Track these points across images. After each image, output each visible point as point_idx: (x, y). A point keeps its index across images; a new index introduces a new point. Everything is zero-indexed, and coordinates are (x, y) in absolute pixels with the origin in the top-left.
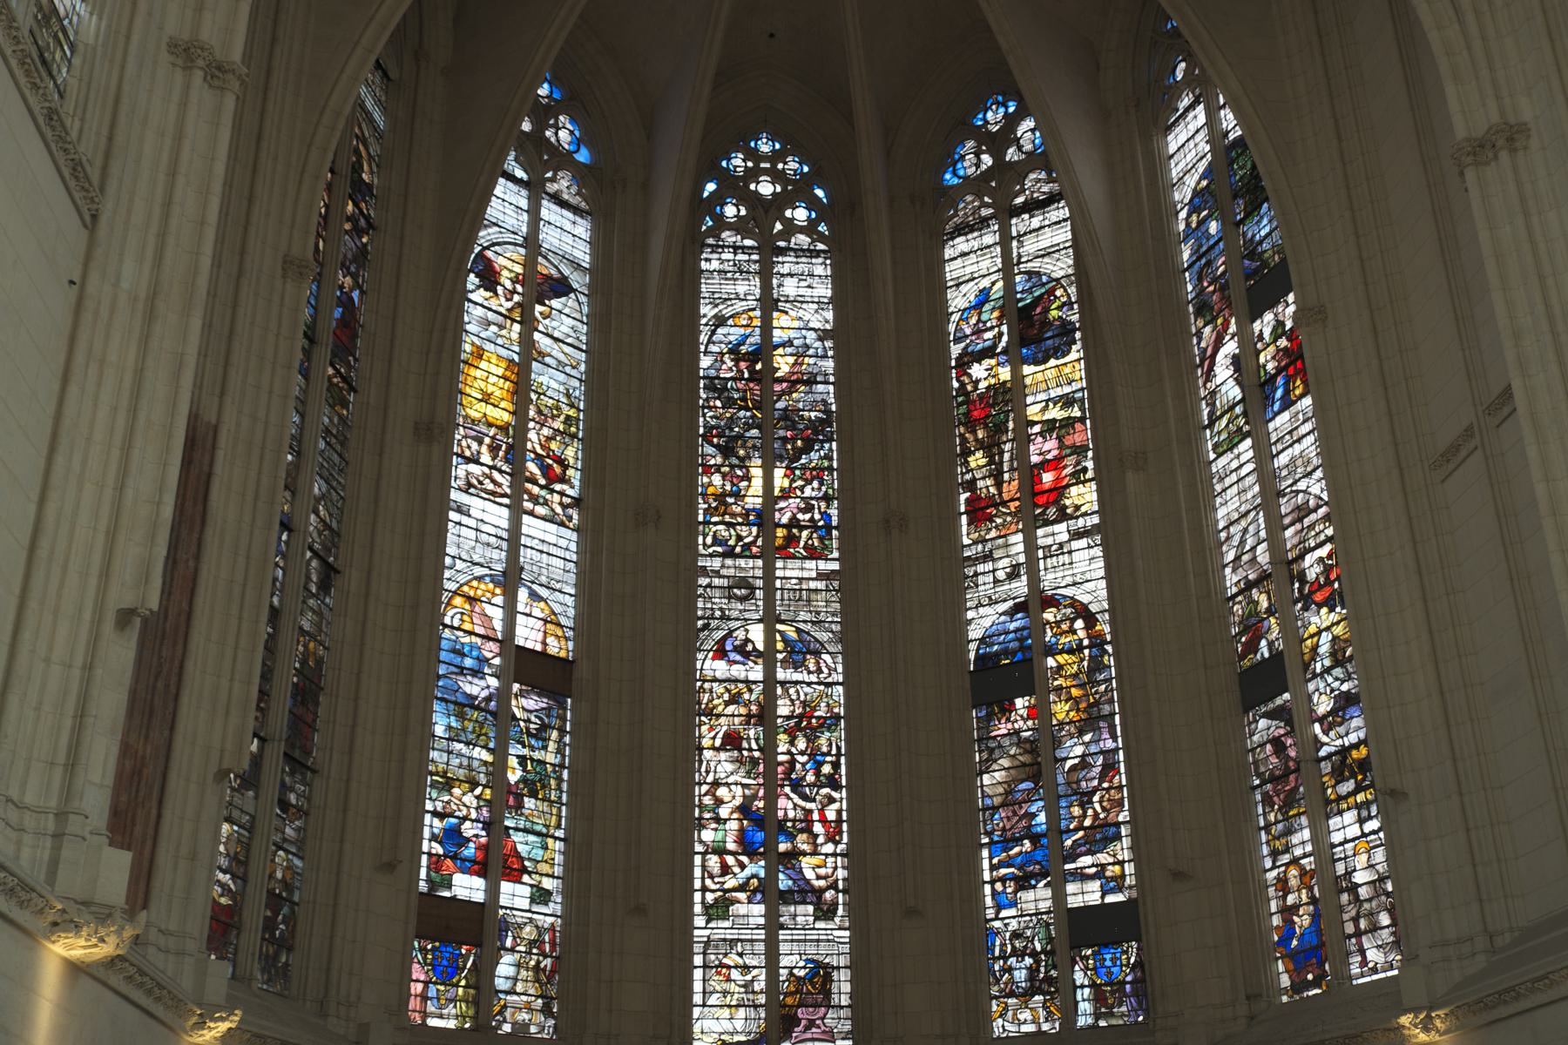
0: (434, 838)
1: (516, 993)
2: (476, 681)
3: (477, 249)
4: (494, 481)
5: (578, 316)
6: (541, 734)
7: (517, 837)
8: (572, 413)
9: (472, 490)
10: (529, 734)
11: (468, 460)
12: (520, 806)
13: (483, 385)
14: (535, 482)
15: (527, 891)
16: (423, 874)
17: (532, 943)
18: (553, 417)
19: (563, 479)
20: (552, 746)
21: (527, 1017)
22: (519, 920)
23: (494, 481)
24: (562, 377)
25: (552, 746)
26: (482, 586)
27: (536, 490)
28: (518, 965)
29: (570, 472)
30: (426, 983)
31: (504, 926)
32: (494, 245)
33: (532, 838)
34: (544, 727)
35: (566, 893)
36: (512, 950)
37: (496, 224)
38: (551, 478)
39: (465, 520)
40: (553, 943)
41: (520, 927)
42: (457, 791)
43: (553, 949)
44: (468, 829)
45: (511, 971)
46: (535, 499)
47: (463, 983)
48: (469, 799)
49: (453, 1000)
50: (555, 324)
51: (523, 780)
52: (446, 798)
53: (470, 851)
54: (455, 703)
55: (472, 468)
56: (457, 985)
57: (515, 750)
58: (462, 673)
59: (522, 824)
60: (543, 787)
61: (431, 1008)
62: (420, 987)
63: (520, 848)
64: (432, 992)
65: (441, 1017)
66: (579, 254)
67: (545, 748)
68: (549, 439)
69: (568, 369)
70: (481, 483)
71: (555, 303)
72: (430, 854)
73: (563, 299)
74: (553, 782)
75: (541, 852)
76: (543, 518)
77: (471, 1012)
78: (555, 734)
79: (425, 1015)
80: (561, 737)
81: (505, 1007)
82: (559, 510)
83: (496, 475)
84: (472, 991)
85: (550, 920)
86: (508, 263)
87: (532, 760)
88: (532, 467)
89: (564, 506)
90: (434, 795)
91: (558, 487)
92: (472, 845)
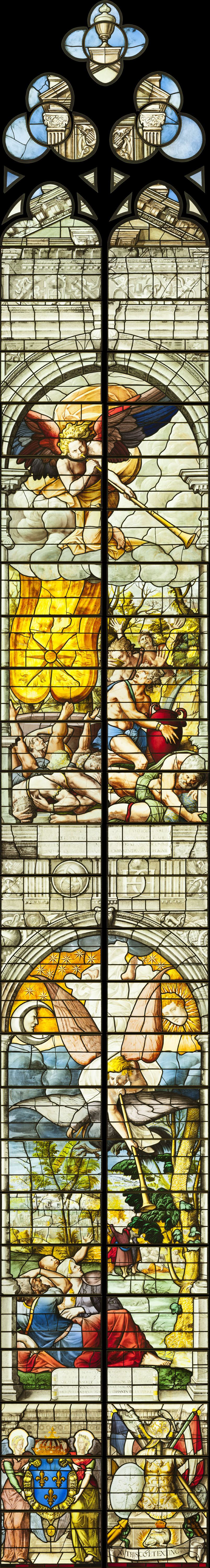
0: (20, 1328)
1: (142, 1510)
2: (65, 1100)
3: (13, 413)
4: (74, 791)
5: (192, 449)
6: (162, 1152)
7: (129, 1304)
8: (188, 626)
9: (41, 817)
10: (142, 1155)
11: (30, 773)
12: (134, 1259)
13: (42, 639)
14: (129, 767)
16: (7, 1376)
18: (156, 648)
19: (177, 746)
20: (181, 1165)
23: (74, 791)
24: (166, 573)
25: (181, 1165)
26: (64, 958)
27: (128, 779)
29: (190, 729)
30: (27, 1513)
32: (44, 391)
33: (156, 1302)
34: (166, 1141)
37: (44, 352)
38: (155, 748)
39: (31, 866)
42: (48, 1261)
43: (198, 1446)
44: (70, 1309)
46: (130, 797)
48: (67, 1266)
50: (148, 483)
51: (137, 1224)
52: (32, 1274)
53: (74, 1336)
54: (37, 1139)
55: (39, 782)
57: (118, 1182)
58: (44, 1096)
59: (137, 1288)
60: (169, 1227)
62: (18, 1518)
63: (138, 1319)
64: (35, 1521)
66: (185, 331)
67: (170, 1170)
68: (148, 687)
69: (177, 554)
70: (52, 800)
71: (148, 446)
72: (15, 1349)
73: (162, 432)
74: (184, 1216)
75: (172, 1319)
76: (147, 822)
78: (185, 1147)
80: (195, 1150)
82: (172, 800)
83: (76, 779)
85: (190, 1408)
86: (71, 413)
87: (149, 1192)
88: (123, 745)
89: (179, 790)
90: (15, 1273)
91: (169, 762)
92: (76, 1327)
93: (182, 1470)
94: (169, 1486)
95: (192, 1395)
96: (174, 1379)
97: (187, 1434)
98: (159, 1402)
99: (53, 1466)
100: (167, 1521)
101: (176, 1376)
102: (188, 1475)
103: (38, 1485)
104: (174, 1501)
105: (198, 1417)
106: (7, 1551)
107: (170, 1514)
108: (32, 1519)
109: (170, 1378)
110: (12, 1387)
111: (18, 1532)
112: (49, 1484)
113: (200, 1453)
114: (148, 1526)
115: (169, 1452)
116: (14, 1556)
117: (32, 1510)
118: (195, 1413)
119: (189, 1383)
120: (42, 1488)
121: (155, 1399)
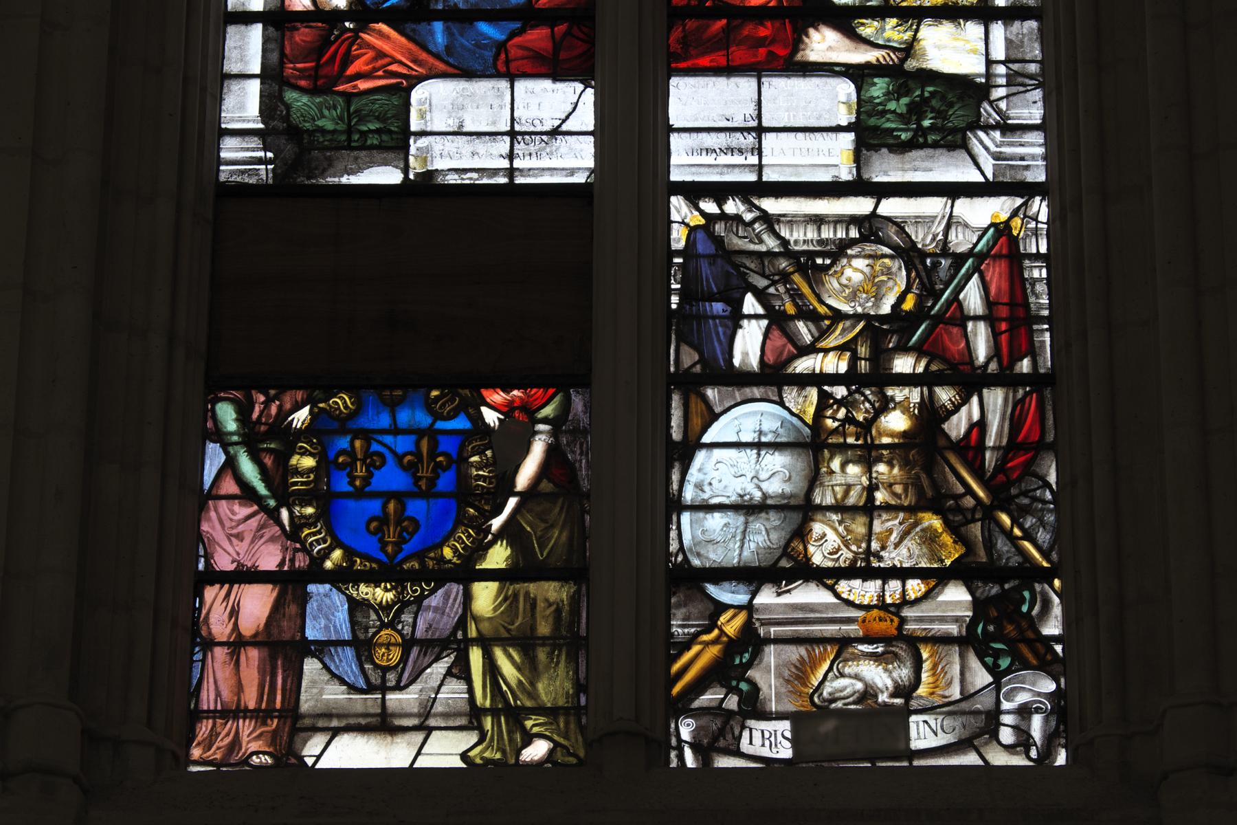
15: (835, 100)
17: (881, 334)
21: (880, 677)
22: (801, 237)
28: (813, 445)
30: (291, 585)
31: (722, 272)
35: (1056, 81)
36: (773, 377)
40: (1009, 314)
41: (811, 266)
45: (776, 474)
47: (498, 557)
49: (453, 644)
56: (467, 573)
61: (319, 688)
65: (383, 725)
77: (553, 687)
79: (291, 723)
81: (752, 640)
84: (552, 591)
85: (981, 213)
93: (957, 426)
94: (912, 483)
95: (988, 165)
96: (916, 110)
97: (973, 298)
98: (859, 187)
99: (404, 417)
100: (907, 612)
101: (925, 101)
102: (981, 447)
103: (343, 485)
104: (930, 539)
105: (1014, 241)
106: (204, 728)
107: (915, 587)
108: (312, 607)
109: (899, 105)
110: (255, 142)
111: (253, 655)
112: (391, 478)
113: (1025, 365)
114: (830, 630)
115: (903, 364)
116: (236, 743)
117: (316, 573)
118: (1001, 230)
119: (976, 124)
120: (360, 494)
121: (846, 173)
